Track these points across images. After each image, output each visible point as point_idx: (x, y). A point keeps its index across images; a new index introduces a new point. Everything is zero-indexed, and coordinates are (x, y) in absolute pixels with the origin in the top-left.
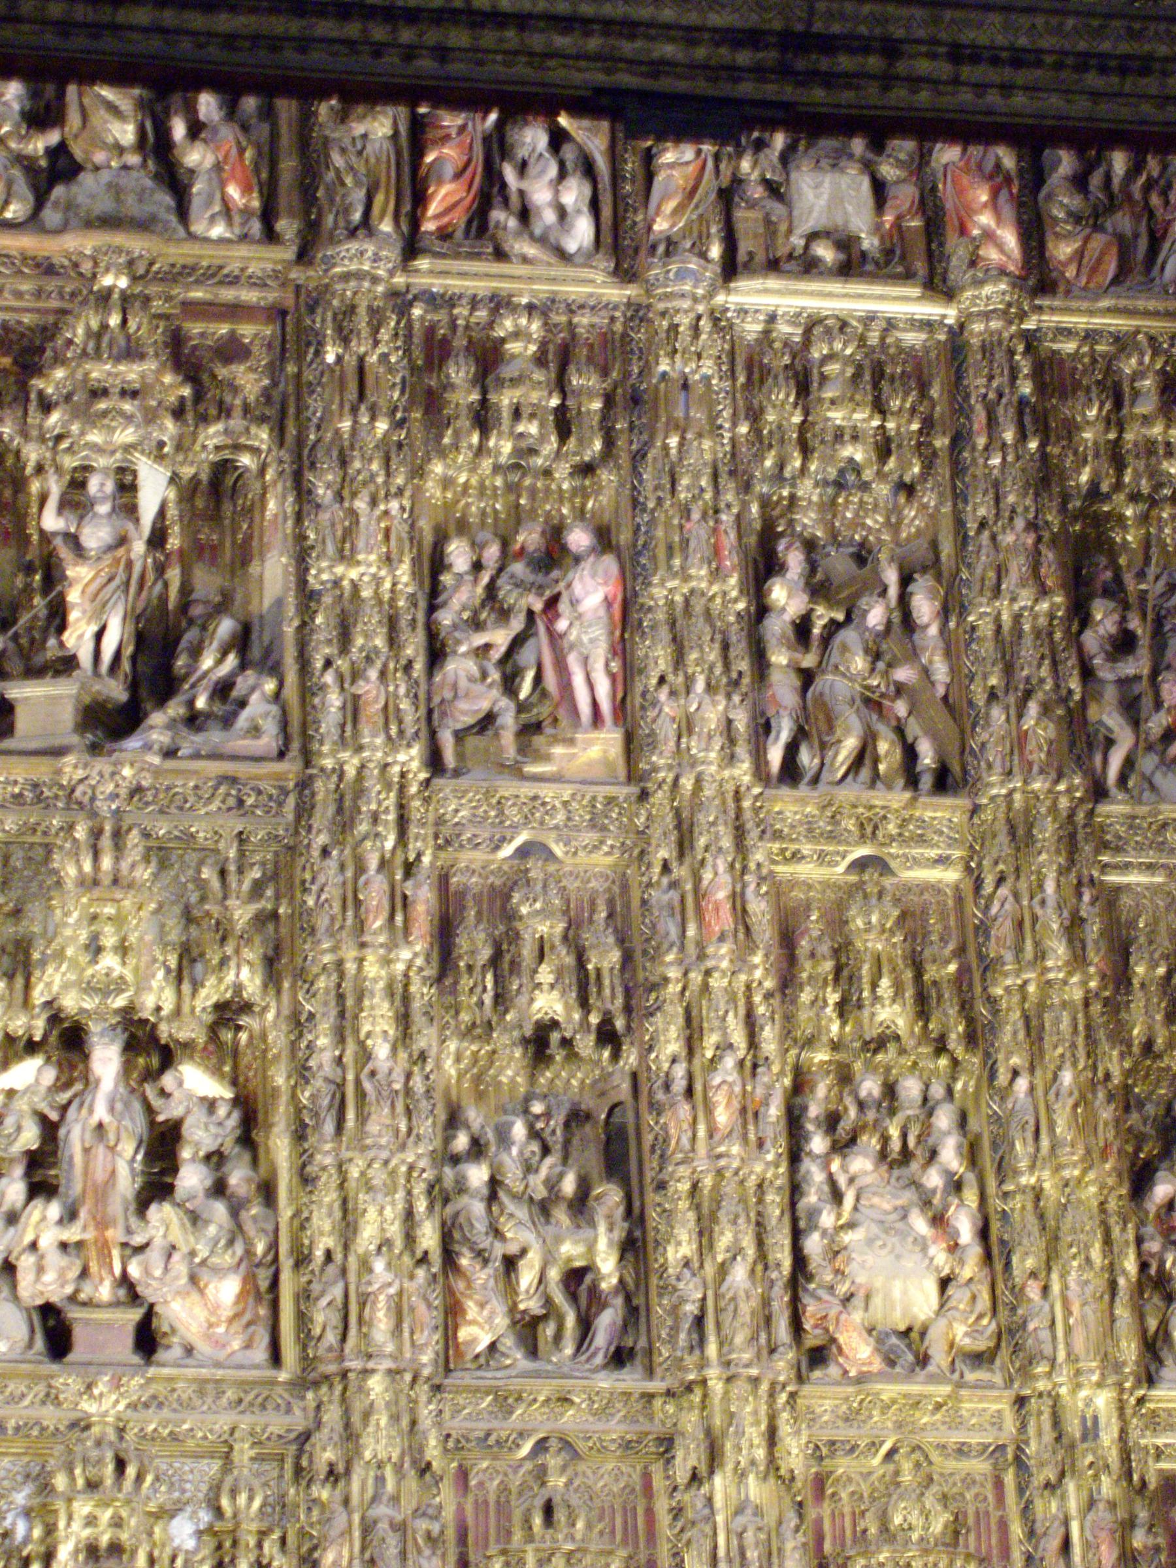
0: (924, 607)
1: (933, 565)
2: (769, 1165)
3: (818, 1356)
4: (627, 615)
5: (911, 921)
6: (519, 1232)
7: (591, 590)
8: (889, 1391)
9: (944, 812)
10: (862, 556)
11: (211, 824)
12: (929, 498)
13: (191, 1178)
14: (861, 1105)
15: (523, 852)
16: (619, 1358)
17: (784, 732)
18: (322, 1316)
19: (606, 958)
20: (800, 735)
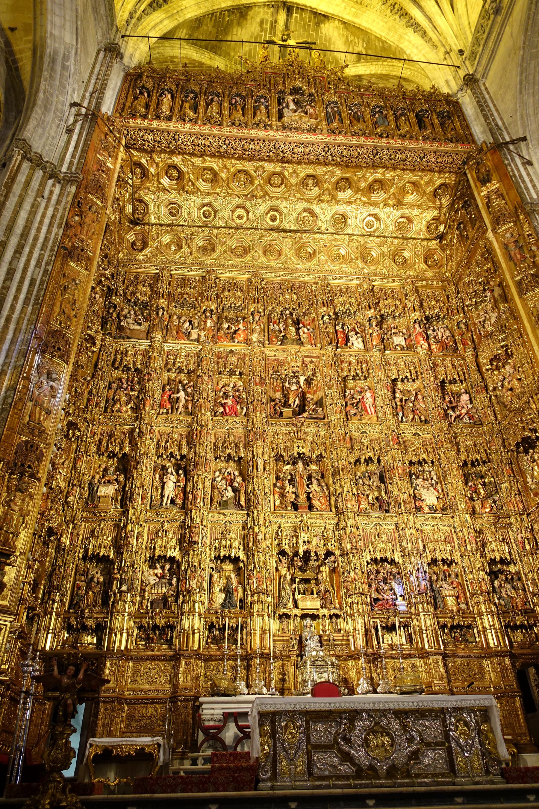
4: (374, 397)
17: (401, 414)
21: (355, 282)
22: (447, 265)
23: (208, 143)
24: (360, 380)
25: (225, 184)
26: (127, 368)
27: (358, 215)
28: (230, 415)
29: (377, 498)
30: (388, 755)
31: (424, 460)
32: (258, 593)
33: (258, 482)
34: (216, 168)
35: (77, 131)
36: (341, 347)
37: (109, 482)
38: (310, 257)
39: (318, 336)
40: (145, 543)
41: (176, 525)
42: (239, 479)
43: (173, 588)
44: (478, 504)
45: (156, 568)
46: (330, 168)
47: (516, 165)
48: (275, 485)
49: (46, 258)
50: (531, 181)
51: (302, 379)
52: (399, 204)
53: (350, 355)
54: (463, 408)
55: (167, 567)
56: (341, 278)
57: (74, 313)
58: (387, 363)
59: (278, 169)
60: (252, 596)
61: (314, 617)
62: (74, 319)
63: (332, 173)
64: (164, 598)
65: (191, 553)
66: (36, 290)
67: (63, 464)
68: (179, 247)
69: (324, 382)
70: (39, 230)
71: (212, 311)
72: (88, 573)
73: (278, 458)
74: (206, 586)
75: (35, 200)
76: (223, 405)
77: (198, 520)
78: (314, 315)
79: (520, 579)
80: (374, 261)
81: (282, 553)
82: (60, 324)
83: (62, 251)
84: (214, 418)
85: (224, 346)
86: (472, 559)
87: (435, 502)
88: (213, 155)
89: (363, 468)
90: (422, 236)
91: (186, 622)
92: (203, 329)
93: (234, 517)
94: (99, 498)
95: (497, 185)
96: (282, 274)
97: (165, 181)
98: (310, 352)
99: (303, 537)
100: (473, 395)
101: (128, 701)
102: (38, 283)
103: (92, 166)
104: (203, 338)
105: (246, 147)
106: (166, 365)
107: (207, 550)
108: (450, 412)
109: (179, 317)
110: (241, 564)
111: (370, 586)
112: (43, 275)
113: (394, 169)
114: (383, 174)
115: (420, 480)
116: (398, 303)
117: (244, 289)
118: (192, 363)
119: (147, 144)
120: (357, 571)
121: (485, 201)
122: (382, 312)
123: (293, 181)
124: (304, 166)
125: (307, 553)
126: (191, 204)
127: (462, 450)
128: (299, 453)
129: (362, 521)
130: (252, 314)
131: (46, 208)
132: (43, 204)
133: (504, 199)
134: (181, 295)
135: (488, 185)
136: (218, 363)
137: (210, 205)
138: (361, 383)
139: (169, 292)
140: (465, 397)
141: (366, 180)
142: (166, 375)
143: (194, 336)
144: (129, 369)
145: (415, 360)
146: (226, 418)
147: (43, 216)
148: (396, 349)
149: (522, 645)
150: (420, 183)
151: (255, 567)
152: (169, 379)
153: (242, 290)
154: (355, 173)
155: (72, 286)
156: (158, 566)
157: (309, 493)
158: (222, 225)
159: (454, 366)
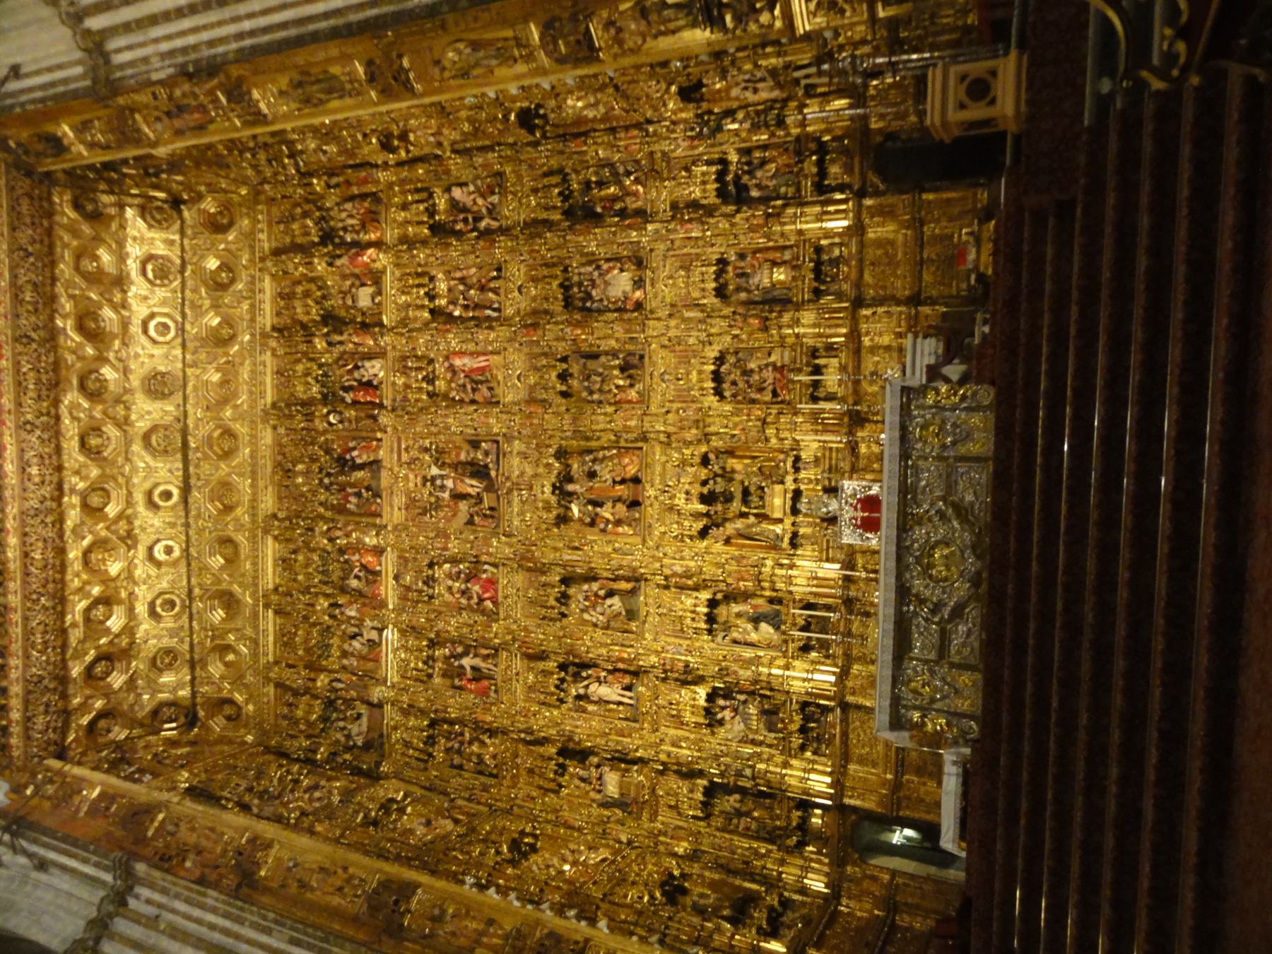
0: (458, 275)
1: (449, 272)
4: (462, 354)
8: (648, 287)
10: (450, 290)
12: (434, 273)
15: (519, 380)
17: (488, 312)
18: (631, 436)
20: (490, 308)
21: (268, 356)
22: (225, 191)
23: (41, 628)
24: (433, 372)
25: (113, 585)
26: (430, 740)
27: (149, 355)
28: (496, 591)
29: (623, 369)
30: (958, 553)
31: (561, 285)
32: (760, 581)
33: (598, 564)
34: (84, 604)
35: (42, 852)
36: (381, 397)
37: (600, 779)
38: (228, 433)
39: (364, 434)
40: (687, 734)
41: (663, 687)
42: (595, 586)
43: (750, 699)
44: (632, 204)
45: (723, 719)
46: (63, 410)
47: (22, 91)
48: (604, 531)
49: (255, 919)
50: (50, 70)
51: (435, 471)
52: (121, 281)
53: (394, 384)
55: (721, 702)
56: (263, 383)
57: (340, 871)
58: (403, 322)
59: (75, 500)
60: (763, 589)
62: (351, 870)
63: (74, 406)
64: (764, 712)
65: (701, 673)
66: (306, 938)
67: (573, 852)
68: (228, 648)
69: (439, 433)
70: (212, 927)
71: (331, 605)
72: (728, 813)
73: (563, 519)
74: (748, 653)
75: (163, 932)
76: (481, 600)
77: (654, 659)
78: (329, 437)
80: (227, 322)
81: (703, 533)
82: (356, 896)
83: (245, 890)
84: (502, 616)
85: (389, 591)
86: (716, 232)
88: (62, 615)
89: (575, 383)
90: (177, 237)
91: (797, 686)
92: (362, 620)
93: (650, 601)
94: (622, 795)
95: (66, 128)
96: (261, 484)
97: (117, 680)
98: (392, 451)
99: (680, 501)
100: (453, 180)
101: (898, 774)
102: (295, 934)
103: (99, 826)
104: (376, 623)
105: (40, 565)
106: (422, 681)
107: (697, 644)
108: (483, 224)
109: (345, 654)
110: (719, 596)
111: (753, 401)
112: (283, 925)
113: (53, 298)
114: (65, 317)
115: (594, 293)
116: (299, 289)
117: (292, 546)
118: (416, 643)
119: (53, 724)
120: (731, 425)
121: (99, 151)
122: (318, 318)
123: (95, 472)
124: (65, 457)
125: (704, 499)
126: (153, 635)
127: (544, 215)
128: (553, 493)
129: (656, 399)
130: (331, 540)
131: (173, 911)
132: (170, 916)
133: (91, 121)
134: (308, 650)
135: (66, 142)
136: (418, 602)
137: (152, 605)
138: (440, 368)
139: (306, 667)
140: (457, 193)
141: (80, 345)
142: (437, 680)
143: (374, 635)
144: (429, 737)
145: (398, 273)
146: (500, 599)
147: (188, 917)
148: (380, 304)
149: (848, 169)
150: (77, 248)
151: (724, 581)
152: (444, 676)
153: (295, 552)
154: (68, 368)
155: (299, 873)
156: (719, 716)
157: (614, 482)
158: (185, 583)
159: (405, 207)
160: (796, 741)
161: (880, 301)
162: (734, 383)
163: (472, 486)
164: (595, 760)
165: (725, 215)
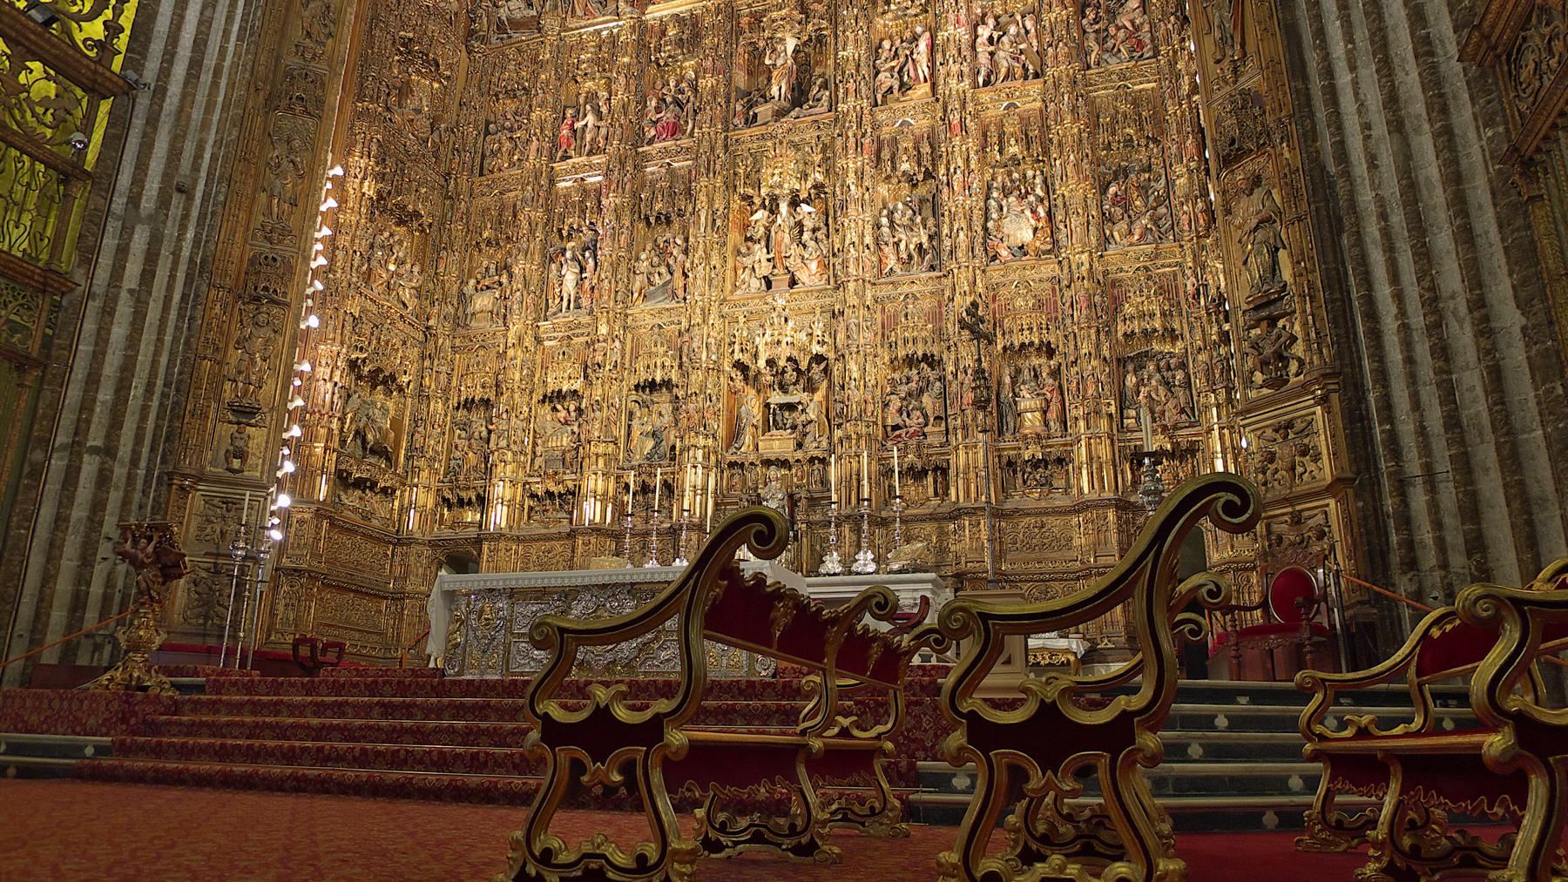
0: (1029, 24)
2: (976, 202)
3: (994, 258)
4: (932, 48)
5: (1024, 121)
6: (902, 235)
7: (923, 45)
9: (1035, 87)
11: (811, 134)
13: (806, 236)
14: (1012, 181)
16: (932, 268)
17: (983, 73)
19: (926, 149)
54: (1118, 28)
61: (784, 464)
79: (1183, 366)
87: (1026, 235)
160: (539, 489)
161: (996, 538)
162: (909, 380)
163: (779, 88)
164: (504, 280)
165: (1098, 346)
